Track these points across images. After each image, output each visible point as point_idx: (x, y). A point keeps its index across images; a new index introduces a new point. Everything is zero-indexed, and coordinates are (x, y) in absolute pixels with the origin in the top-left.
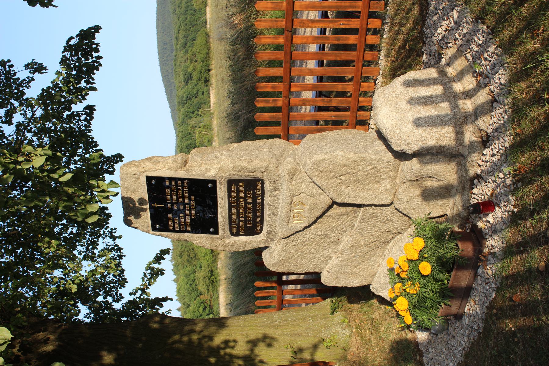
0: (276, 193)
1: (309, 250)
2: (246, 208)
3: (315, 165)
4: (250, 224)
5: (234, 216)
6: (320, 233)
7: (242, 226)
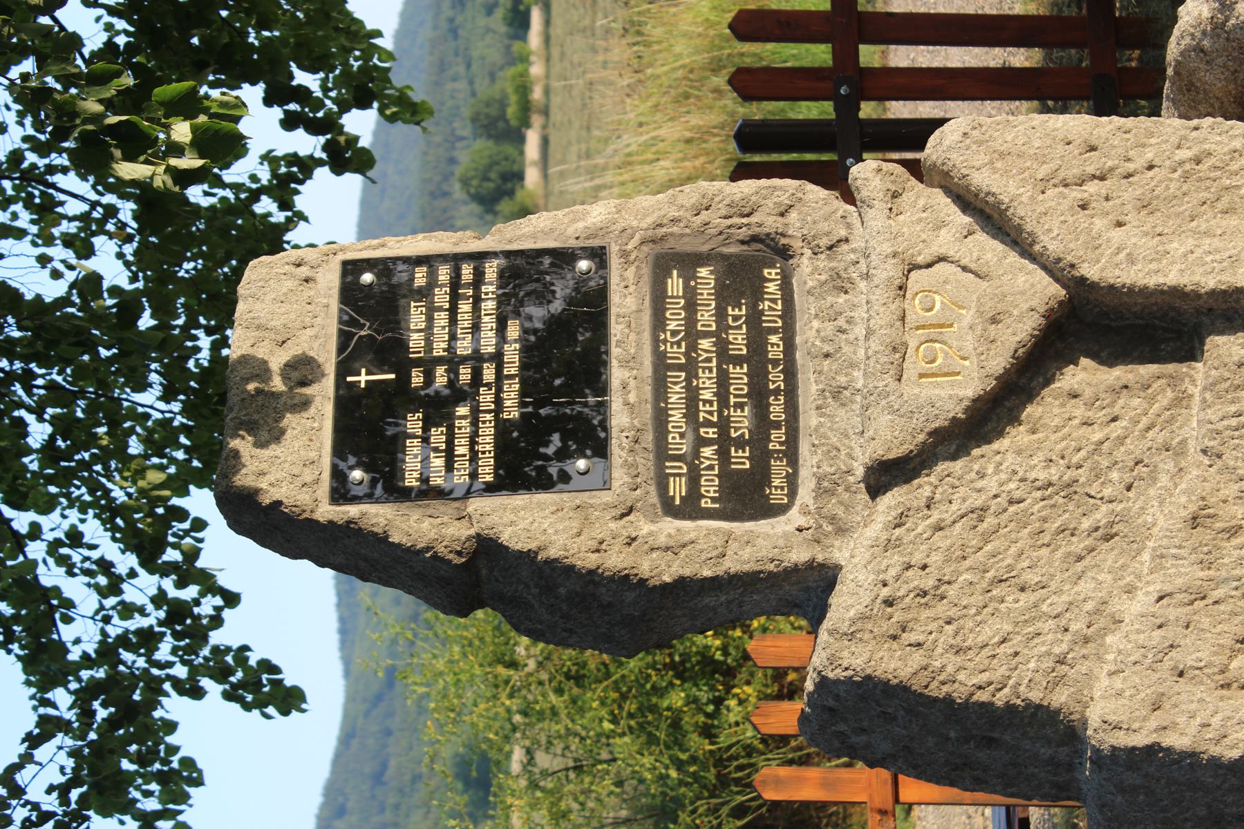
0: (841, 300)
1: (1009, 561)
2: (723, 382)
3: (975, 133)
4: (741, 460)
5: (676, 416)
6: (1042, 475)
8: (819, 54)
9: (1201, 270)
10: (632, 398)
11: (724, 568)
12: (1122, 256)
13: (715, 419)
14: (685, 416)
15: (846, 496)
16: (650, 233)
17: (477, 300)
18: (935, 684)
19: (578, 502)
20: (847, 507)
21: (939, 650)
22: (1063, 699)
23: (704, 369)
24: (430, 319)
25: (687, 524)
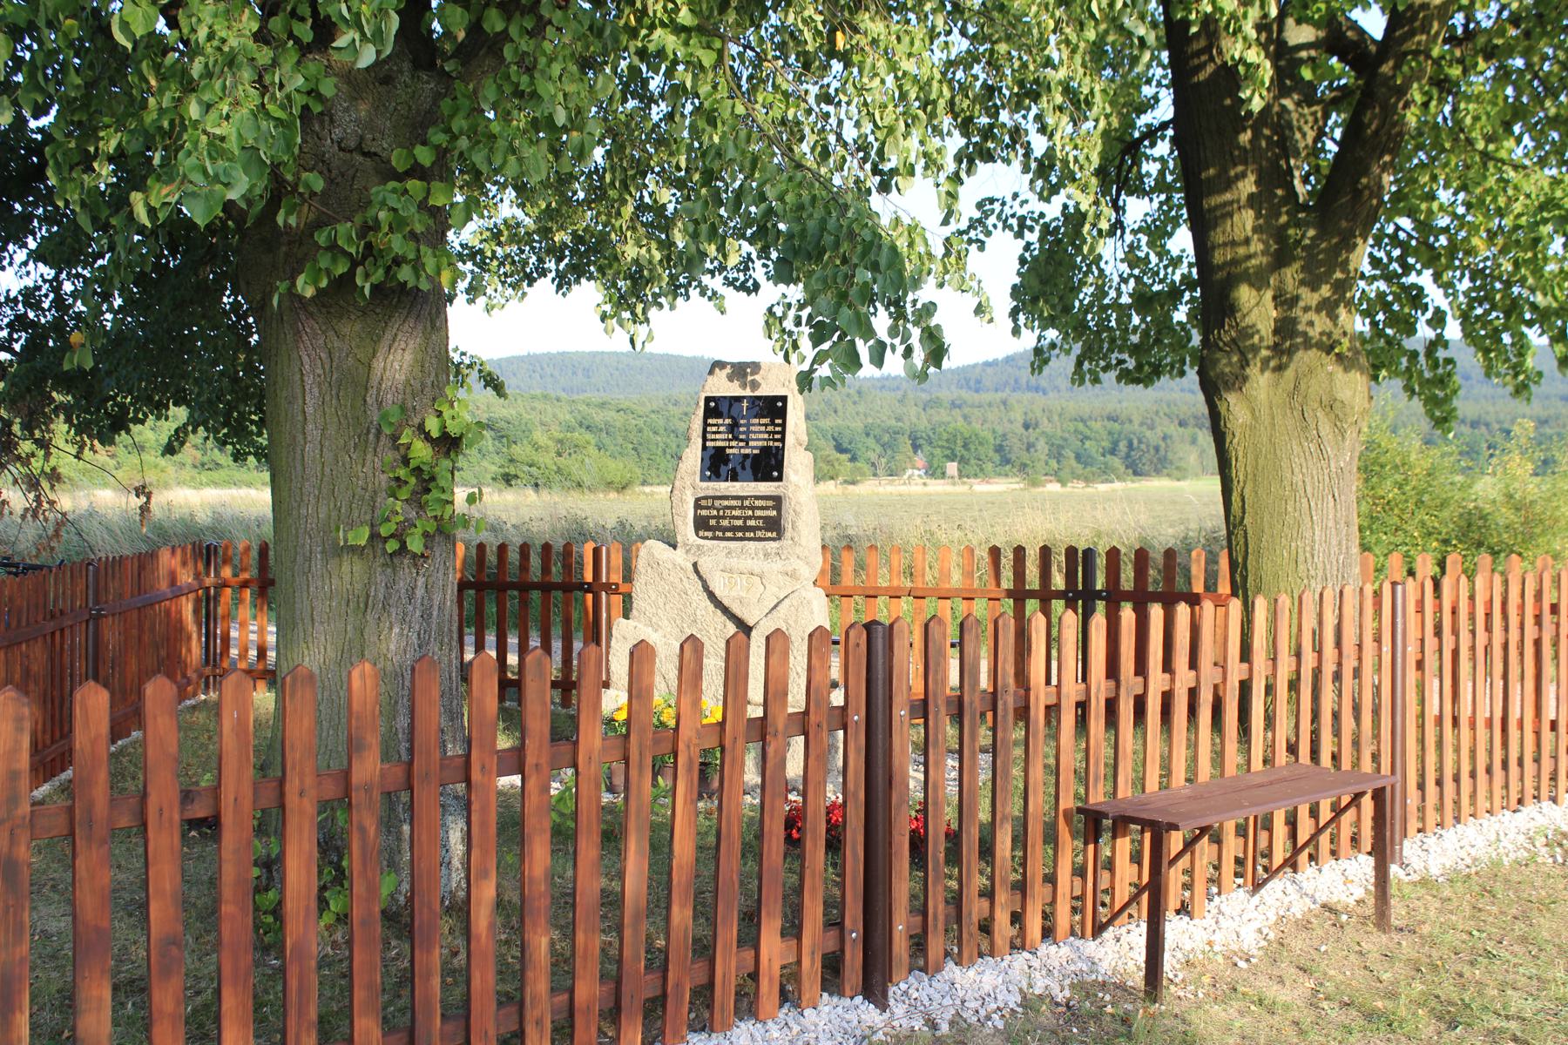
4: (713, 522)
5: (726, 503)
8: (1100, 583)
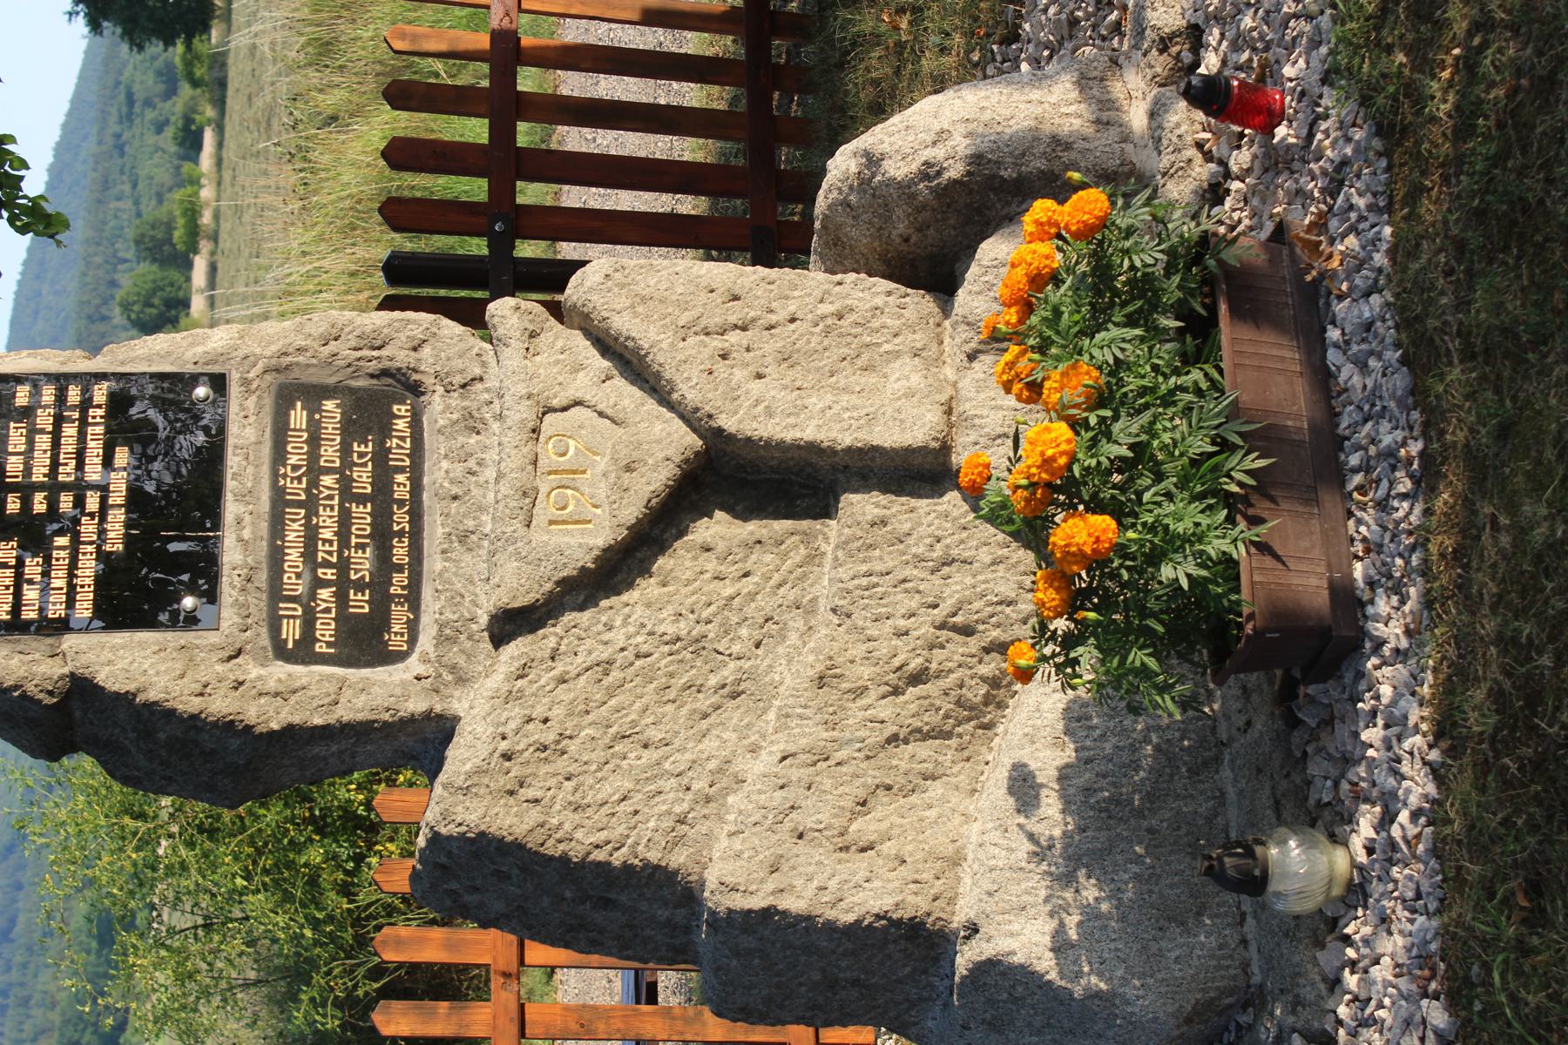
0: (472, 441)
1: (633, 717)
2: (345, 520)
4: (360, 603)
5: (293, 555)
6: (671, 630)
7: (327, 610)
8: (474, 189)
9: (838, 426)
10: (246, 534)
11: (336, 716)
12: (760, 408)
13: (334, 560)
14: (302, 554)
15: (468, 644)
16: (274, 361)
17: (83, 423)
18: (549, 844)
19: (183, 642)
20: (469, 656)
21: (557, 807)
22: (682, 860)
23: (325, 506)
24: (31, 443)
25: (299, 669)
